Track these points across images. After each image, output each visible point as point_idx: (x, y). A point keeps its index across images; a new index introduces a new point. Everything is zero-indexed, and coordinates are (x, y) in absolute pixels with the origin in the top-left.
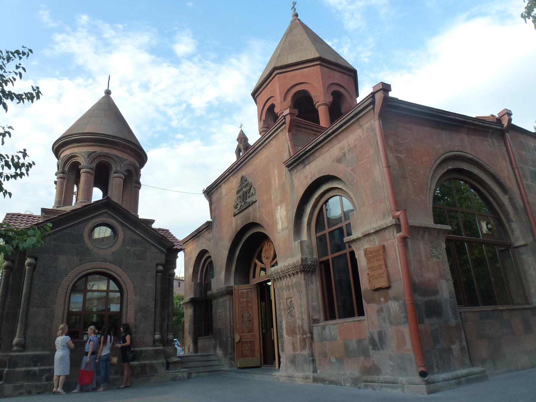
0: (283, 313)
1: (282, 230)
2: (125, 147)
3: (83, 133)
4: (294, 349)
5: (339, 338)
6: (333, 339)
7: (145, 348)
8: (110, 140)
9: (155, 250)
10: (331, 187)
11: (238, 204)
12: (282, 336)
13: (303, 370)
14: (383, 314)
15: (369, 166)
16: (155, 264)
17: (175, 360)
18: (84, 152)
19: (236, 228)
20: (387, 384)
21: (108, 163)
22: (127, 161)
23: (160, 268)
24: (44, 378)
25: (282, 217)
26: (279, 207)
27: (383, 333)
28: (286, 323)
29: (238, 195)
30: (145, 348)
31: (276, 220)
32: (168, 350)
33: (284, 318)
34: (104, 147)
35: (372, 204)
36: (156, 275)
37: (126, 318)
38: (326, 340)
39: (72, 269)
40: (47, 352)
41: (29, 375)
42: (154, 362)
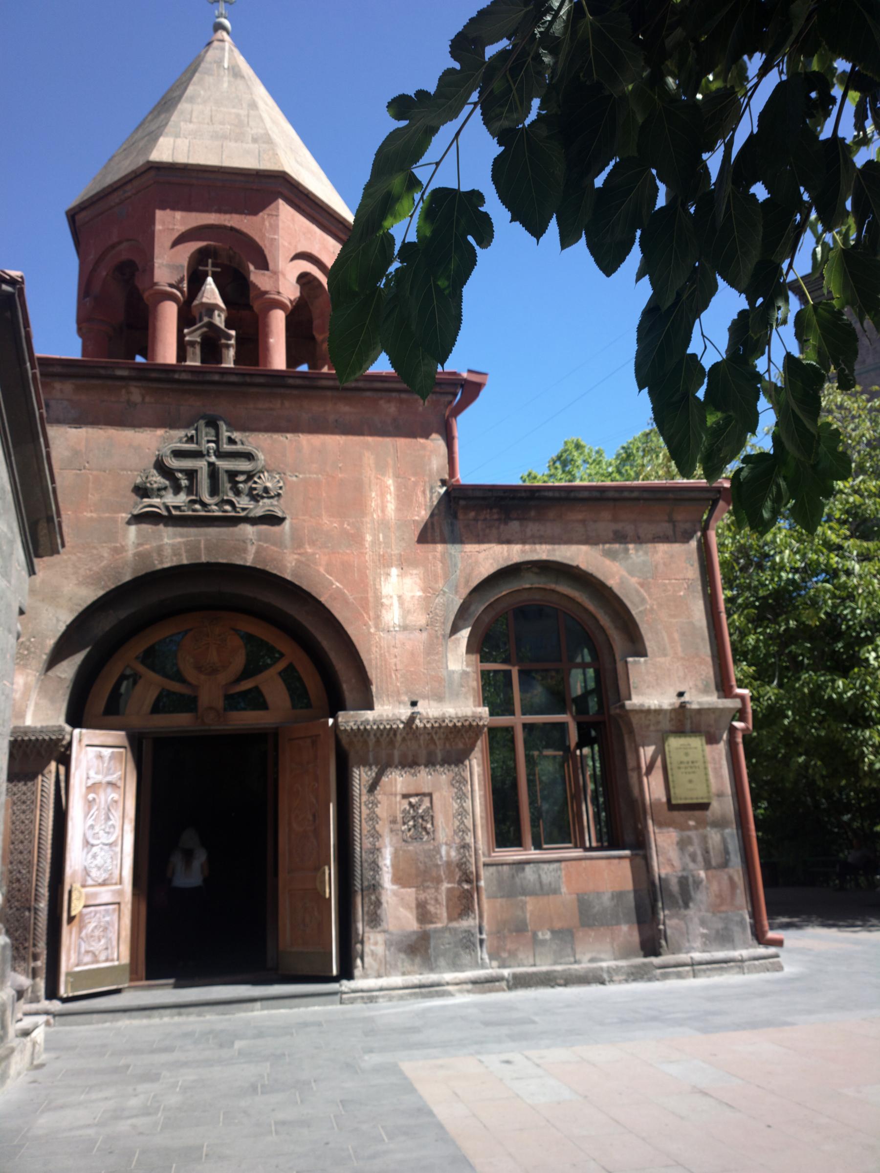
0: (383, 828)
1: (405, 628)
4: (423, 914)
5: (564, 890)
6: (544, 890)
10: (553, 586)
11: (165, 488)
12: (375, 887)
13: (455, 966)
14: (691, 849)
15: (682, 593)
19: (141, 556)
20: (709, 966)
25: (407, 596)
26: (394, 571)
27: (691, 880)
28: (396, 856)
29: (174, 463)
31: (378, 598)
35: (682, 658)
38: (524, 893)
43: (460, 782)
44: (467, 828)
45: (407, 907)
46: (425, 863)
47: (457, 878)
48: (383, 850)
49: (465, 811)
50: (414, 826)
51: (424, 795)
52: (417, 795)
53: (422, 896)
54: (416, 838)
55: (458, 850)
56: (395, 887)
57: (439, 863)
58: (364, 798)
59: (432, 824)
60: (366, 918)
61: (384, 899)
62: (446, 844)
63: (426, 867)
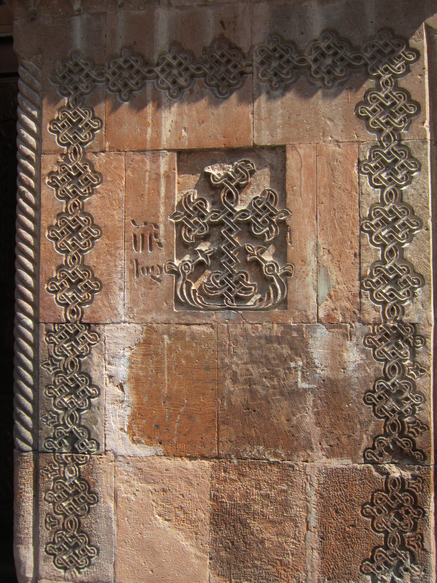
33: (121, 300)
43: (390, 111)
44: (411, 269)
45: (180, 516)
46: (250, 382)
47: (366, 442)
48: (107, 331)
49: (410, 210)
50: (216, 256)
51: (255, 150)
52: (231, 153)
53: (236, 488)
54: (229, 296)
55: (370, 344)
56: (143, 451)
57: (303, 385)
58: (50, 163)
59: (282, 253)
60: (45, 534)
61: (105, 484)
62: (330, 322)
63: (253, 393)
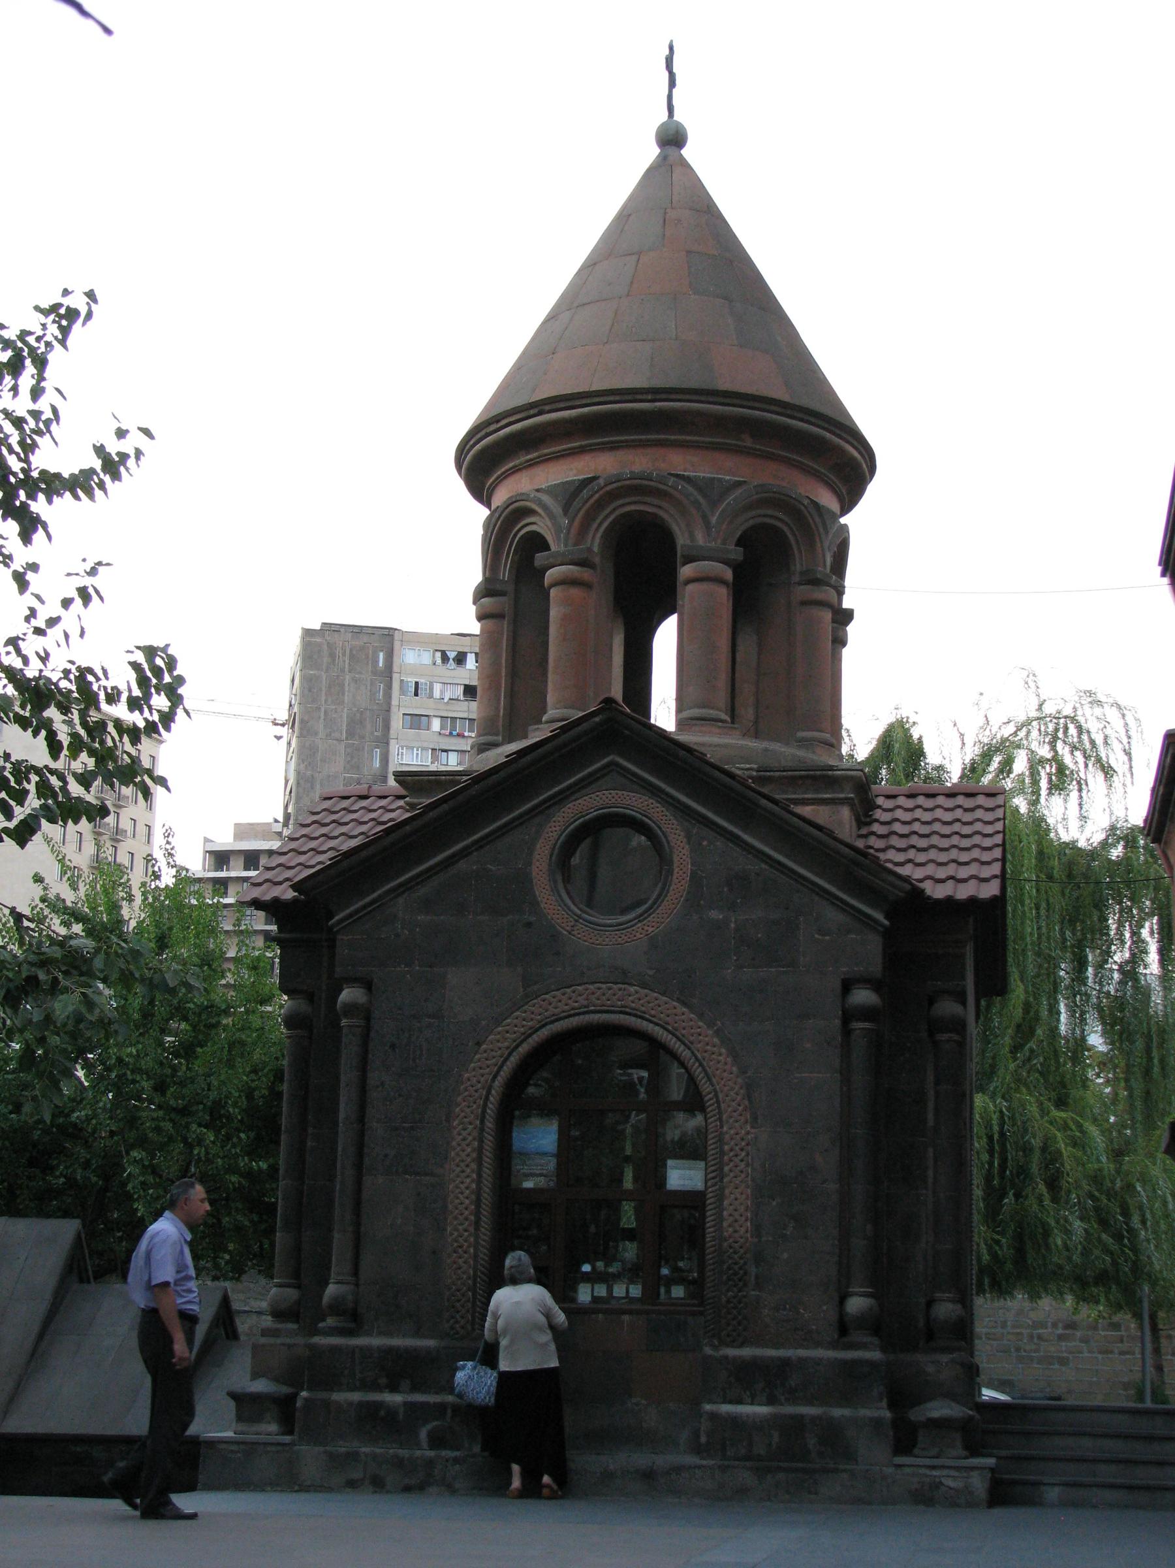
2: (719, 424)
3: (532, 405)
7: (802, 1353)
8: (642, 413)
9: (833, 916)
16: (837, 985)
17: (935, 1414)
18: (550, 491)
21: (655, 515)
22: (739, 491)
23: (863, 996)
24: (423, 1434)
30: (802, 1353)
32: (930, 1369)
34: (628, 445)
36: (847, 1032)
37: (720, 1218)
39: (498, 1022)
40: (431, 1343)
41: (373, 1420)
42: (837, 1412)
